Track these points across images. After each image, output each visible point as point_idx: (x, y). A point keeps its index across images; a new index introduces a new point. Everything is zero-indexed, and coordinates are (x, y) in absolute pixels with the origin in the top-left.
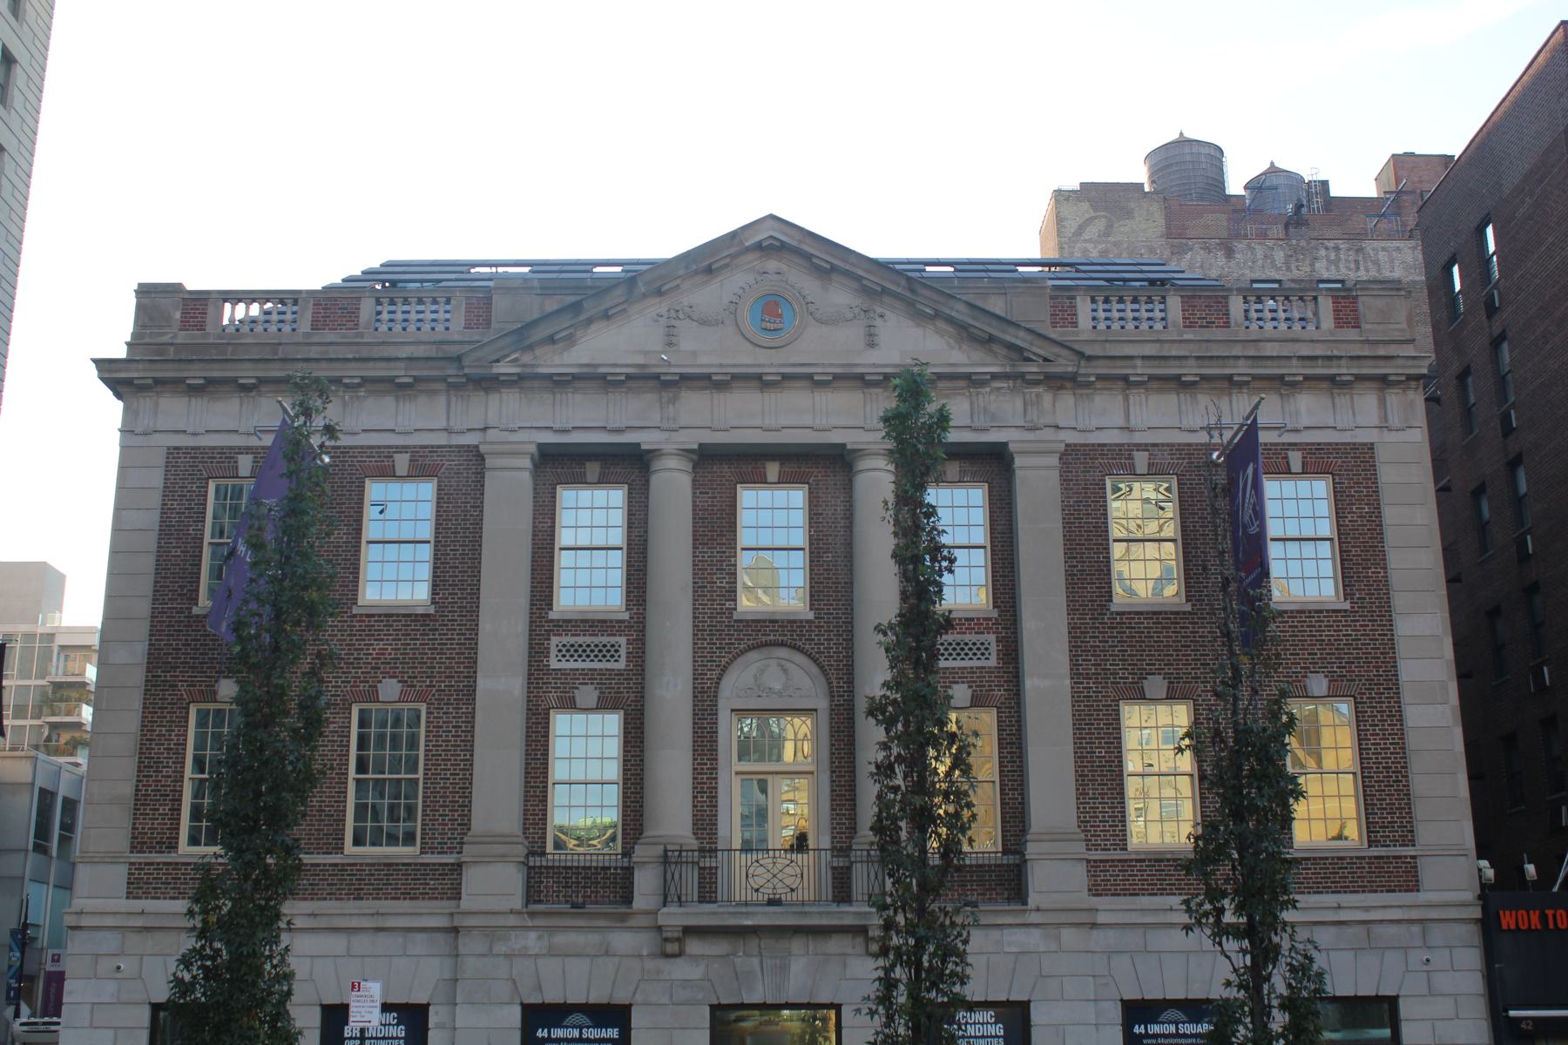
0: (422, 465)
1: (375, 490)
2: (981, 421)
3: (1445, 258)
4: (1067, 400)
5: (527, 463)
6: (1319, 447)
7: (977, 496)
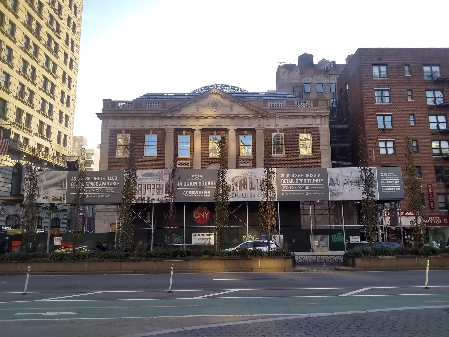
0: (155, 132)
1: (147, 136)
2: (251, 124)
3: (340, 89)
4: (265, 120)
5: (173, 132)
6: (309, 128)
7: (250, 137)
